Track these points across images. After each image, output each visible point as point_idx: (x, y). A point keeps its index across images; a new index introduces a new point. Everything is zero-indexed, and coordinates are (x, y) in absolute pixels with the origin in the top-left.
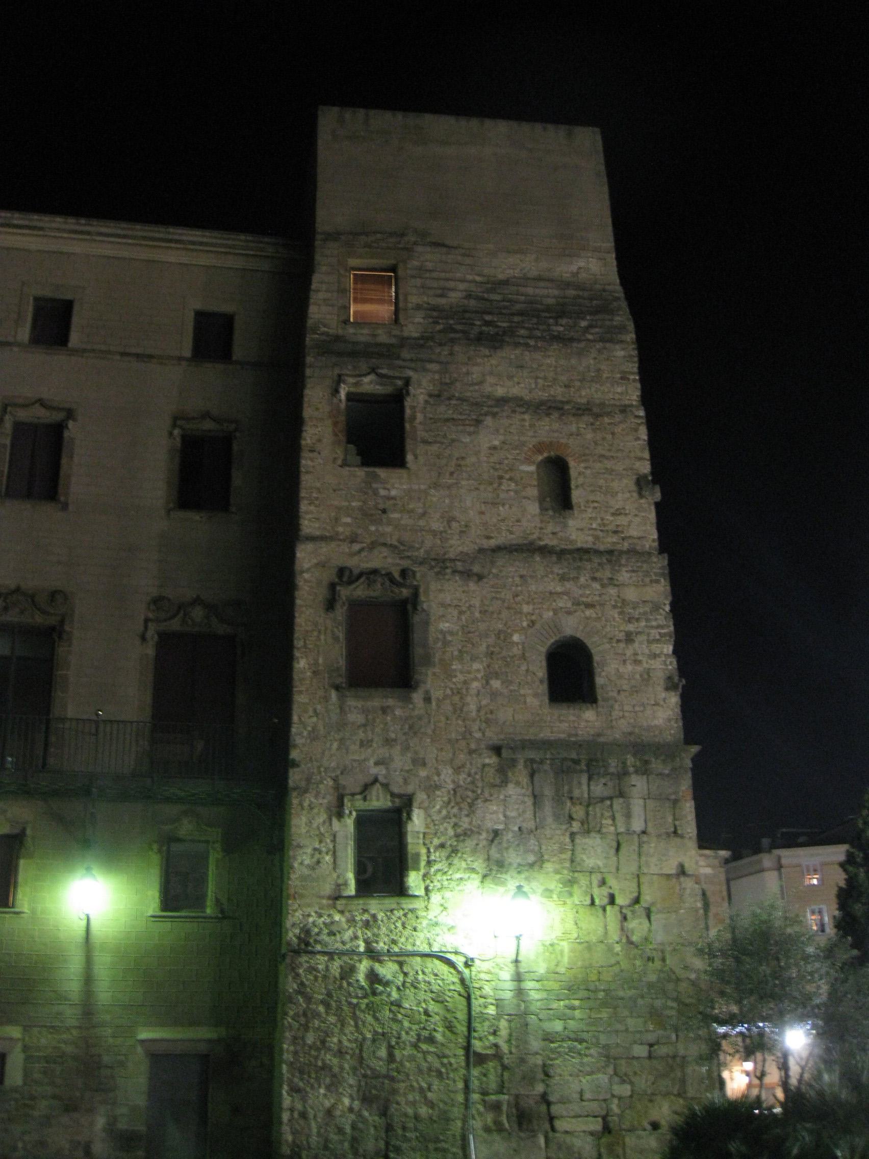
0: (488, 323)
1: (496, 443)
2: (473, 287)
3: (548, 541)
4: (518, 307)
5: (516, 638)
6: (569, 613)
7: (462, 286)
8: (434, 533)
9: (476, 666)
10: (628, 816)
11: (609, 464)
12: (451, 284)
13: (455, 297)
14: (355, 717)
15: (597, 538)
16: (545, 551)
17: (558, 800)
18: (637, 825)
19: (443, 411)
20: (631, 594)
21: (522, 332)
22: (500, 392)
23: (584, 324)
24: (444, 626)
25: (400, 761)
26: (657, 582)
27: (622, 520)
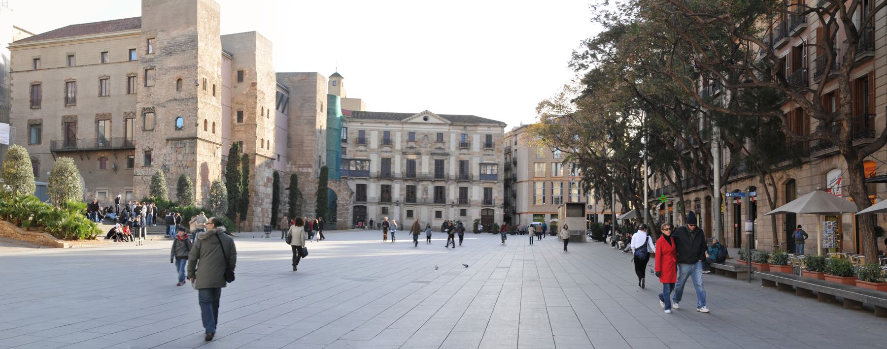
0: (170, 49)
1: (170, 78)
2: (168, 40)
3: (178, 98)
4: (177, 44)
5: (170, 118)
6: (179, 112)
7: (166, 41)
8: (158, 98)
9: (164, 124)
10: (186, 150)
11: (190, 79)
12: (164, 41)
13: (165, 44)
14: (145, 135)
16: (176, 100)
17: (175, 147)
18: (187, 152)
19: (161, 72)
20: (190, 107)
21: (177, 50)
22: (171, 66)
23: (188, 45)
24: (159, 117)
25: (151, 143)
27: (191, 91)
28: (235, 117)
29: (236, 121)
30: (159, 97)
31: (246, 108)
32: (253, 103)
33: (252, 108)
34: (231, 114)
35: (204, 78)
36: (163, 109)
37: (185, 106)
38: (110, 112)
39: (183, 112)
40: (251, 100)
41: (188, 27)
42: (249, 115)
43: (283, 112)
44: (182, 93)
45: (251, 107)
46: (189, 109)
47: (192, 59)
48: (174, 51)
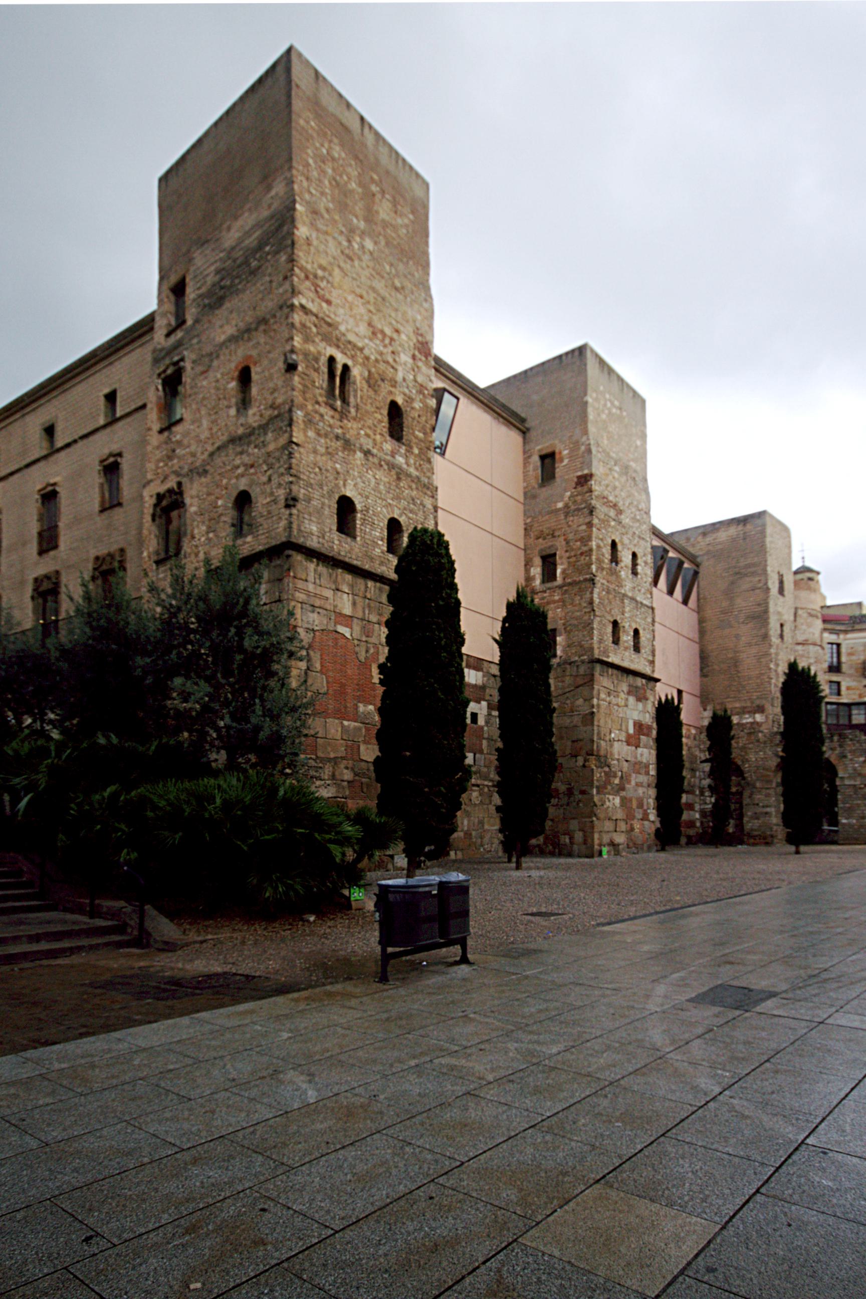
11: (271, 356)
15: (261, 416)
26: (286, 431)
27: (276, 395)
28: (536, 571)
29: (538, 582)
30: (193, 448)
31: (564, 543)
32: (584, 527)
33: (581, 540)
34: (526, 565)
35: (332, 360)
36: (203, 480)
37: (256, 450)
38: (121, 546)
39: (252, 471)
40: (578, 522)
41: (269, 188)
42: (573, 559)
43: (685, 602)
44: (251, 412)
45: (578, 537)
46: (269, 454)
47: (281, 285)
48: (231, 286)
